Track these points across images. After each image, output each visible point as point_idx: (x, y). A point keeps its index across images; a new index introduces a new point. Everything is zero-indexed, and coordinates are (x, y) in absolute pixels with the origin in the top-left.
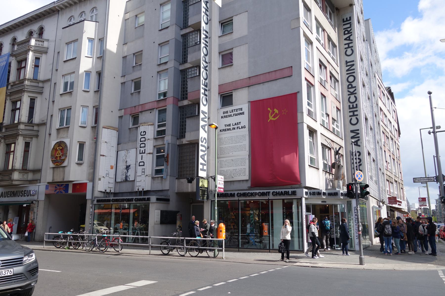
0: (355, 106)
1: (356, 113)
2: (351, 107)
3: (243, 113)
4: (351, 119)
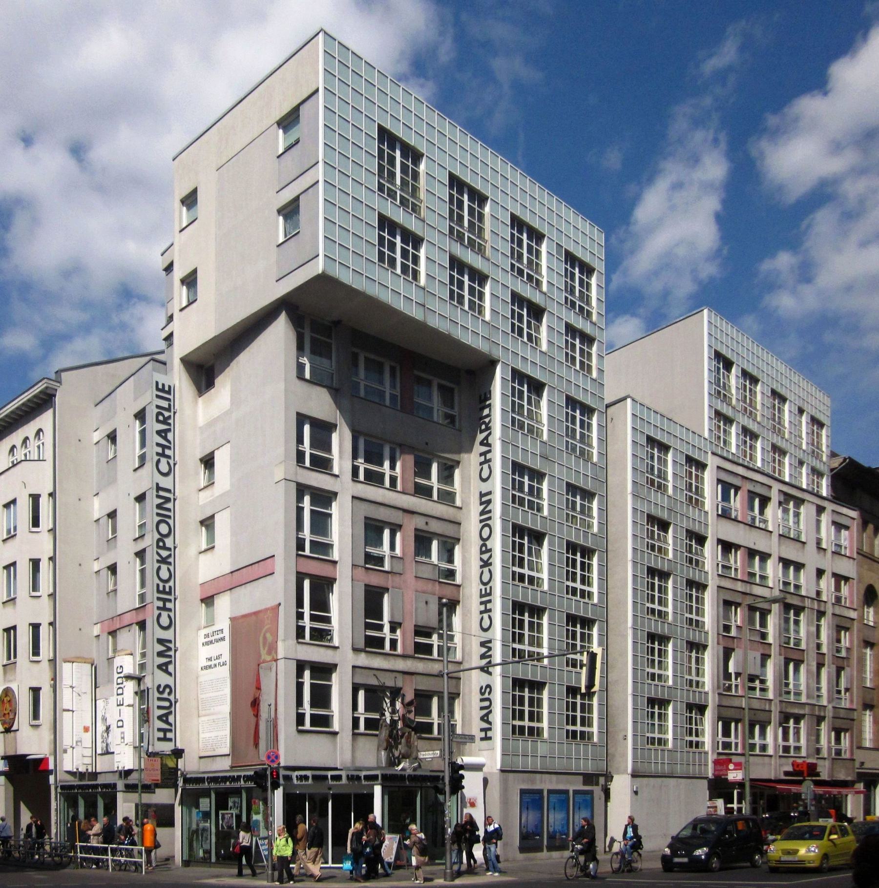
0: (167, 590)
1: (168, 605)
2: (161, 588)
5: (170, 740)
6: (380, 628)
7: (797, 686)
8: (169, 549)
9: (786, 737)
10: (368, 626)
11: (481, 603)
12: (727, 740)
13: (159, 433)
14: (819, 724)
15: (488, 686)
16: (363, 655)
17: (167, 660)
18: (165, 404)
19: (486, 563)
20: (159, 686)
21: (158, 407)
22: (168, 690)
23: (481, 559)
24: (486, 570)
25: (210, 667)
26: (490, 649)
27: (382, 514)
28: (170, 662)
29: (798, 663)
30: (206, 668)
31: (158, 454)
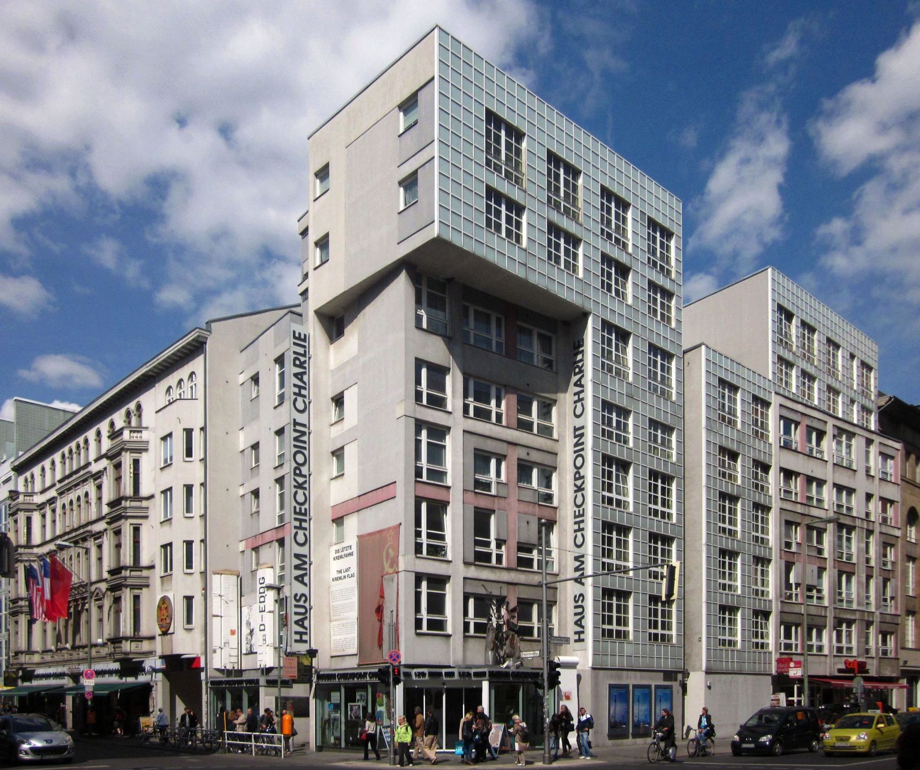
0: (303, 511)
1: (304, 525)
2: (298, 510)
5: (306, 642)
6: (488, 544)
7: (848, 595)
8: (305, 476)
9: (839, 639)
10: (477, 543)
11: (575, 523)
12: (788, 641)
13: (296, 375)
14: (868, 628)
15: (581, 595)
16: (473, 568)
17: (303, 572)
18: (301, 350)
19: (580, 489)
20: (296, 595)
21: (295, 353)
22: (303, 599)
23: (575, 485)
24: (579, 494)
25: (340, 578)
26: (583, 563)
27: (489, 446)
28: (306, 574)
29: (850, 575)
30: (336, 579)
31: (295, 394)
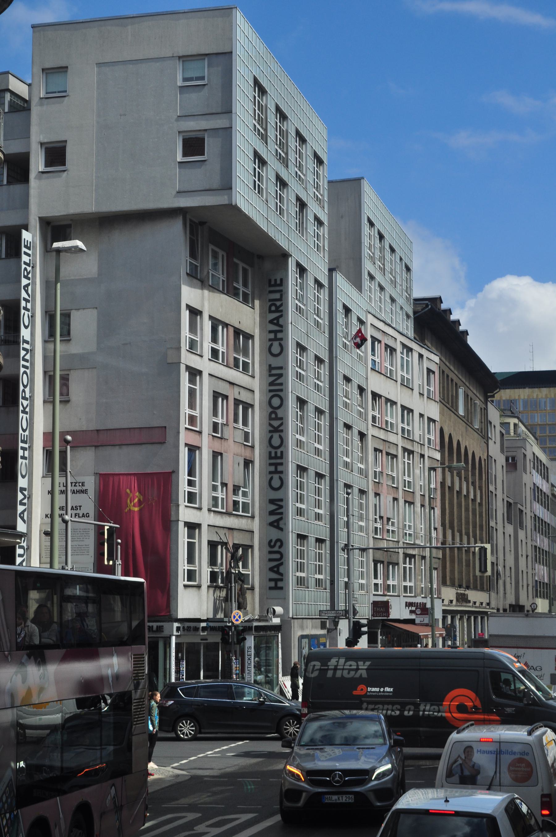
0: (279, 455)
2: (273, 455)
3: (85, 492)
4: (271, 479)
20: (271, 541)
22: (278, 544)
